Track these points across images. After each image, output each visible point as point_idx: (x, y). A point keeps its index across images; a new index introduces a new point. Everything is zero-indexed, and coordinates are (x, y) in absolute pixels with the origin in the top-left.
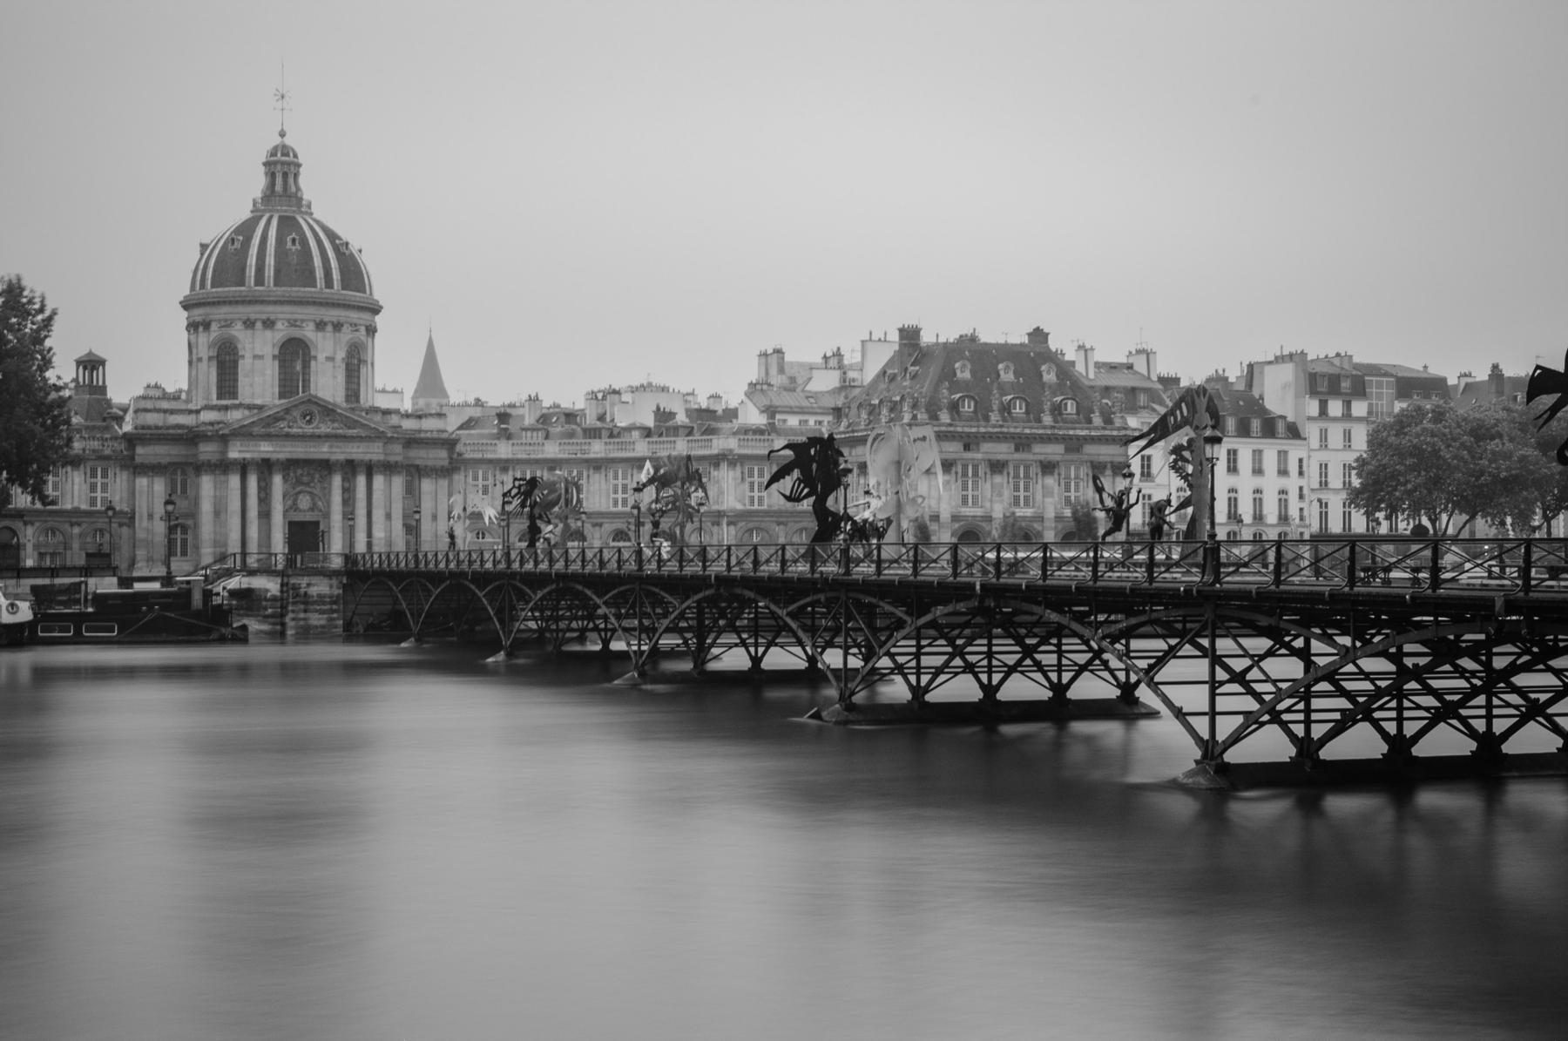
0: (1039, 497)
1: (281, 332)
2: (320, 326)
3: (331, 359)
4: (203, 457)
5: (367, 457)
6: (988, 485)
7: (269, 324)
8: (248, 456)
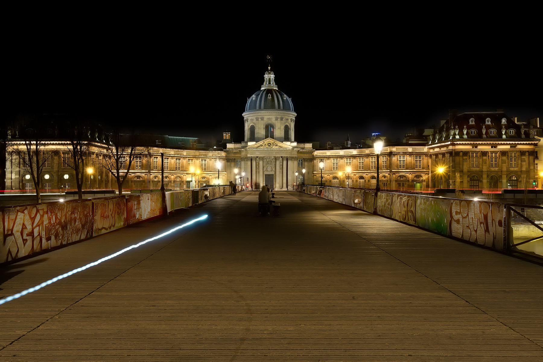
0: (500, 163)
4: (242, 156)
5: (286, 156)
6: (481, 160)
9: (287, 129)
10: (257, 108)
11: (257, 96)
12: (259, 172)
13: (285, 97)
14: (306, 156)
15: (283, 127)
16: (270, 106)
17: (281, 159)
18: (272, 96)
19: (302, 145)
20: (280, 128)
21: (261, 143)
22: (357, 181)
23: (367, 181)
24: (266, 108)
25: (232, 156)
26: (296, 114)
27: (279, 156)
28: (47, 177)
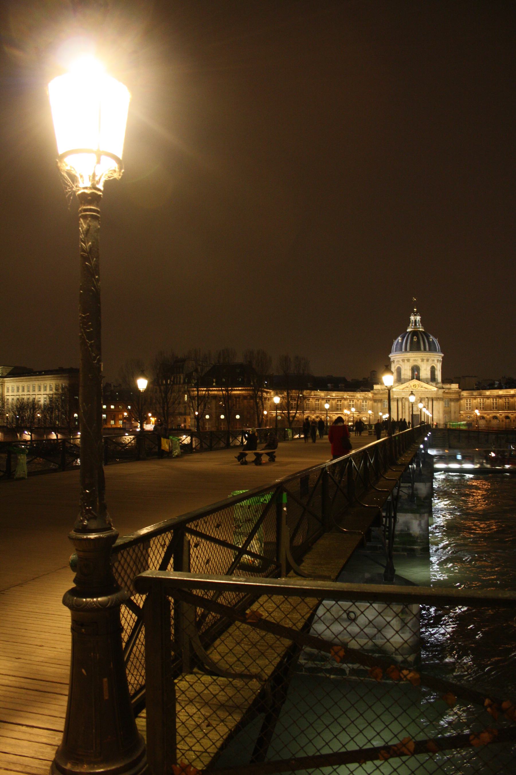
1: (412, 363)
2: (423, 360)
3: (426, 370)
7: (408, 360)
8: (399, 397)
9: (433, 370)
10: (403, 350)
11: (403, 338)
12: (405, 412)
13: (431, 338)
14: (453, 396)
15: (429, 368)
16: (415, 347)
17: (426, 399)
18: (418, 338)
19: (448, 386)
20: (426, 370)
21: (406, 384)
22: (503, 421)
23: (512, 421)
24: (412, 350)
25: (378, 397)
26: (443, 355)
27: (423, 396)
28: (207, 417)
